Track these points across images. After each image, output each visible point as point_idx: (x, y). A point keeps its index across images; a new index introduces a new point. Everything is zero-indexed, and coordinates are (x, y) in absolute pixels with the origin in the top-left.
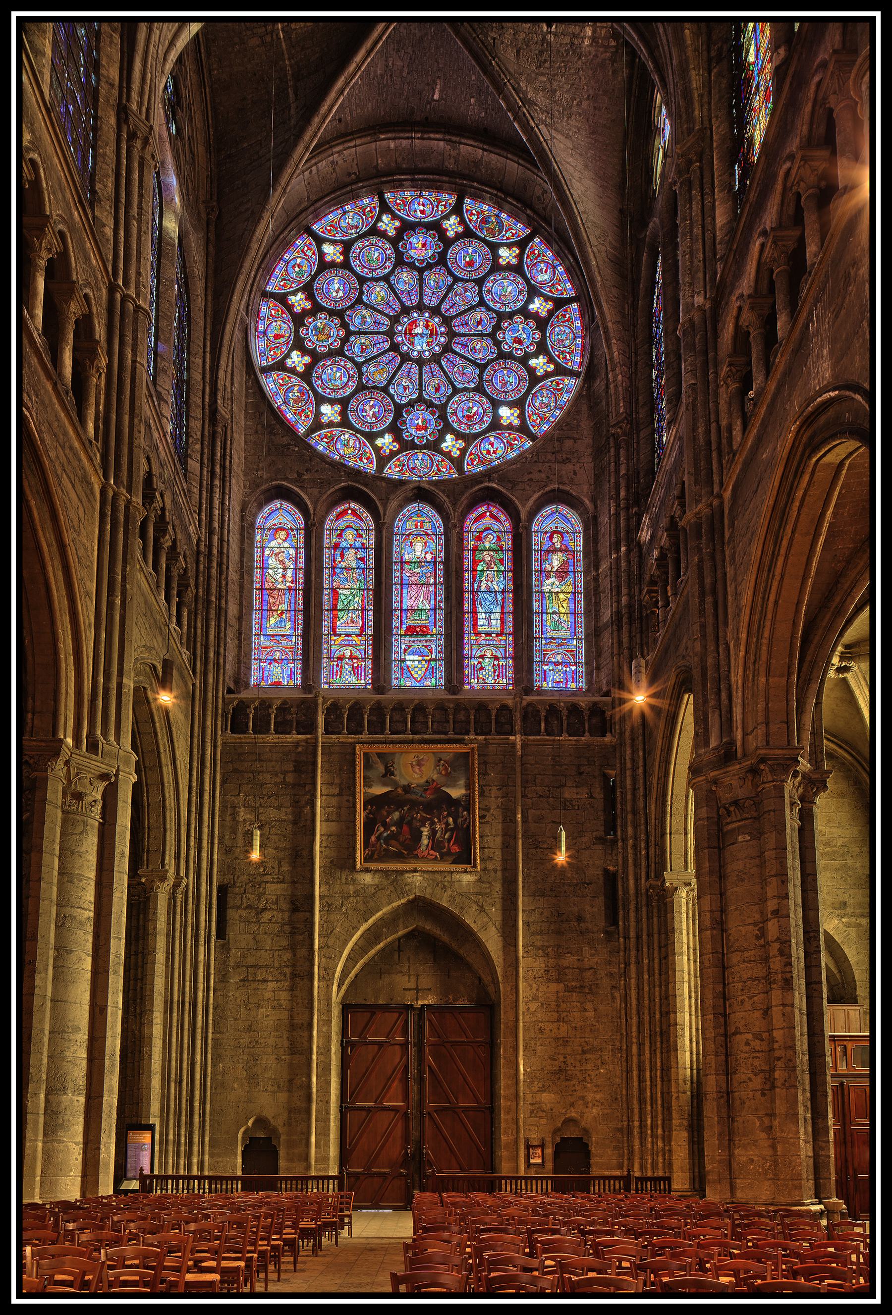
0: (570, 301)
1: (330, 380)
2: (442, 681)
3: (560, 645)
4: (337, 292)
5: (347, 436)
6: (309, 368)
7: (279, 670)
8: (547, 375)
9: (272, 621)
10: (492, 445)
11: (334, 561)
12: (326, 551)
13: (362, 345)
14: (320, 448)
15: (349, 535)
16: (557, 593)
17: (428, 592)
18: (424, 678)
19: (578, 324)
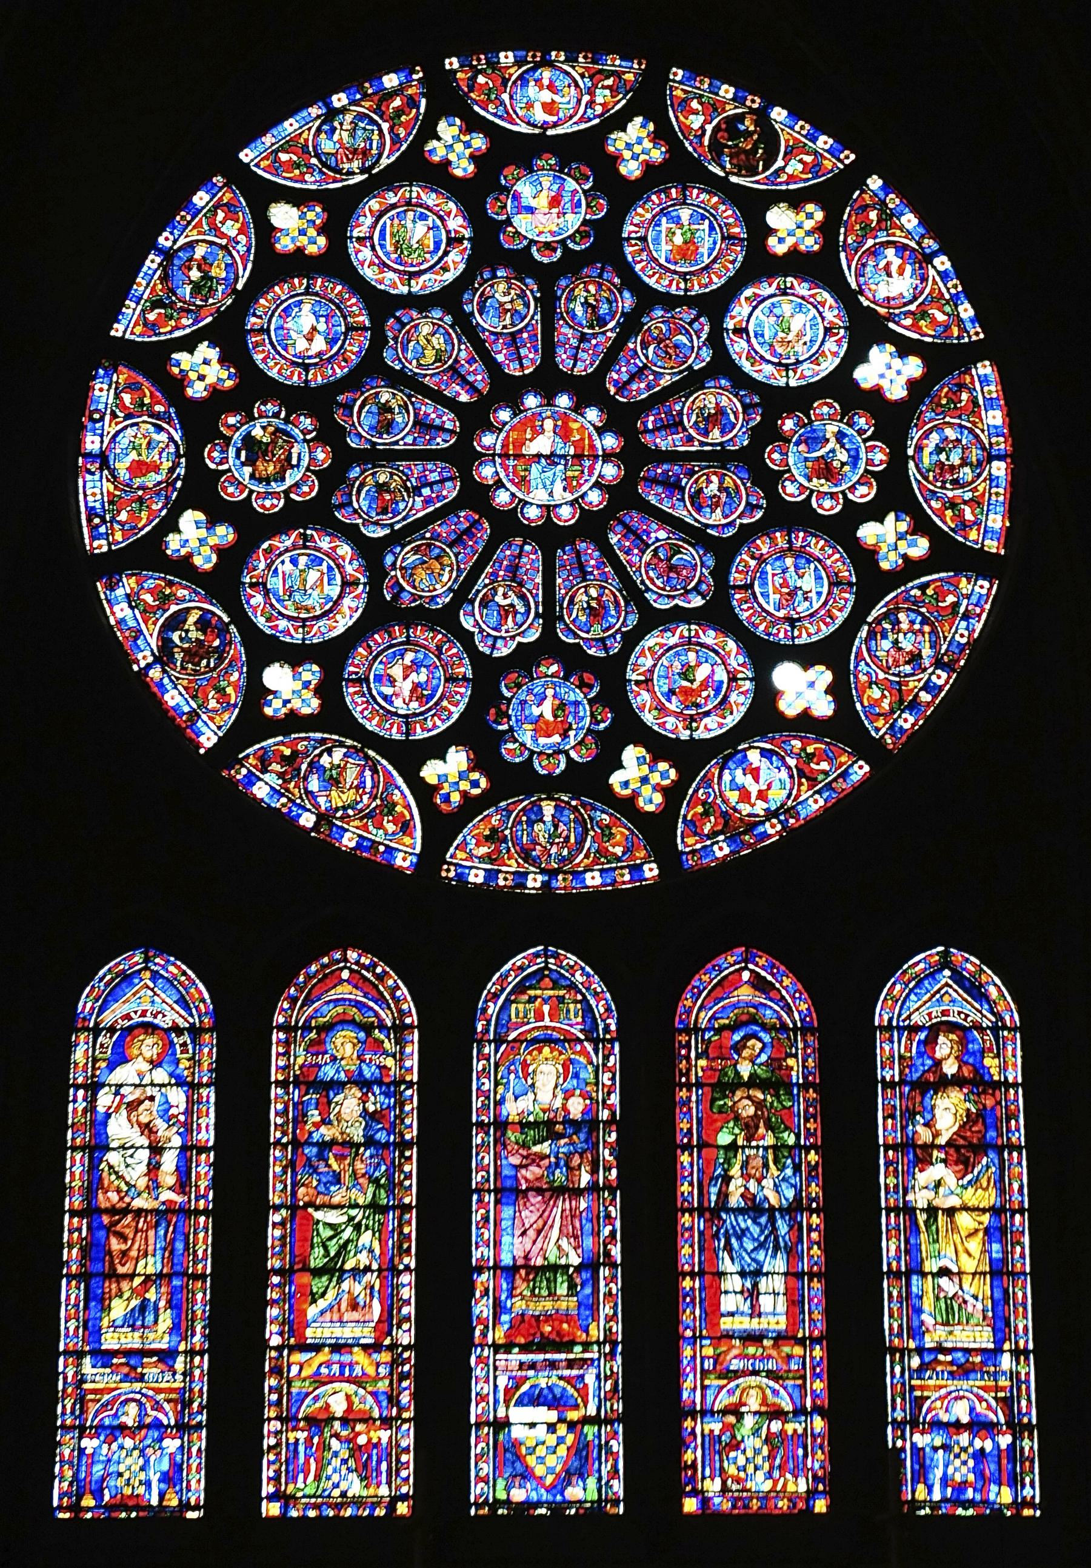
0: (970, 354)
1: (290, 592)
2: (618, 1487)
3: (964, 1371)
4: (310, 339)
5: (338, 754)
6: (233, 559)
7: (134, 1461)
8: (911, 568)
9: (119, 1309)
10: (755, 773)
11: (300, 1119)
12: (275, 1091)
13: (382, 488)
14: (260, 791)
15: (344, 1044)
16: (951, 1212)
17: (574, 1214)
18: (568, 1476)
19: (995, 418)
